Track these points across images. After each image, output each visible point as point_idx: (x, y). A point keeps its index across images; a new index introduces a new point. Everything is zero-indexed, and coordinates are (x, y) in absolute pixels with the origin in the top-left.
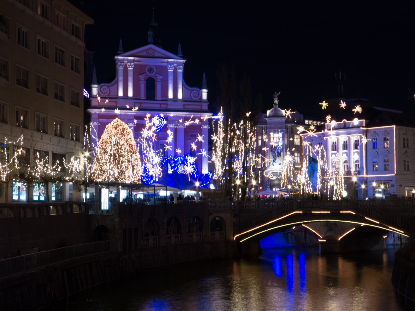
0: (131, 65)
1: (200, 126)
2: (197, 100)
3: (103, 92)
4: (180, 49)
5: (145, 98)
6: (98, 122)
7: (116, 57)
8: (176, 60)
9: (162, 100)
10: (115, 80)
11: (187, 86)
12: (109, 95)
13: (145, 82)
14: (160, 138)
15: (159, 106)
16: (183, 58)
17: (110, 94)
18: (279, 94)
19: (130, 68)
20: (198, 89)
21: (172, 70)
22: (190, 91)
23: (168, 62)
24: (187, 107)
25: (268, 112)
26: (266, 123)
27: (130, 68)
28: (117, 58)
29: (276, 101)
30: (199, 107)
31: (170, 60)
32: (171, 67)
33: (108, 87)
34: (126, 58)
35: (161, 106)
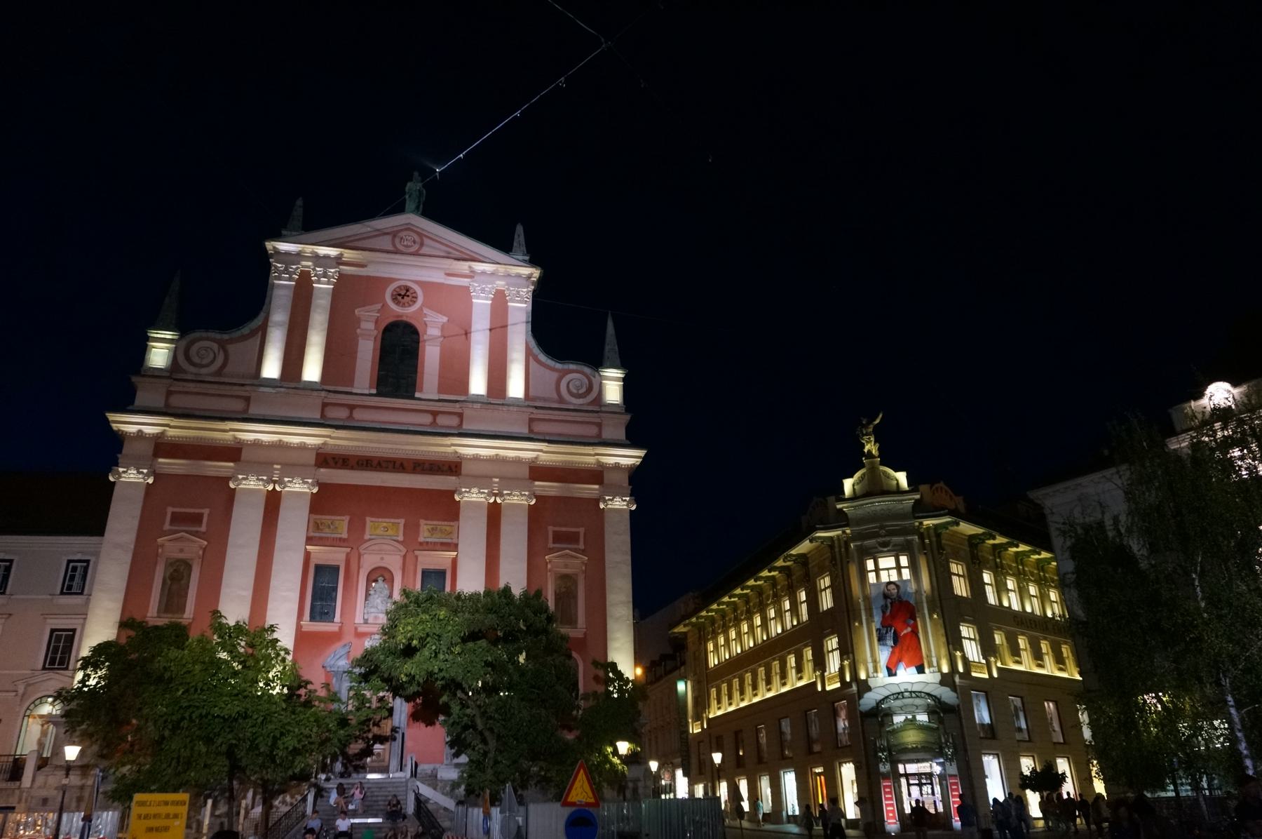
0: (325, 275)
1: (597, 501)
2: (585, 408)
3: (196, 360)
4: (522, 239)
5: (374, 391)
7: (270, 245)
8: (501, 269)
9: (439, 400)
10: (258, 322)
11: (543, 357)
12: (219, 372)
14: (421, 544)
15: (427, 419)
16: (533, 262)
17: (226, 370)
18: (877, 421)
19: (323, 287)
20: (587, 370)
21: (486, 299)
22: (555, 375)
23: (472, 275)
25: (848, 485)
26: (841, 519)
27: (323, 287)
28: (274, 248)
29: (871, 447)
30: (593, 431)
31: (479, 267)
32: (483, 290)
33: (223, 345)
34: (309, 249)
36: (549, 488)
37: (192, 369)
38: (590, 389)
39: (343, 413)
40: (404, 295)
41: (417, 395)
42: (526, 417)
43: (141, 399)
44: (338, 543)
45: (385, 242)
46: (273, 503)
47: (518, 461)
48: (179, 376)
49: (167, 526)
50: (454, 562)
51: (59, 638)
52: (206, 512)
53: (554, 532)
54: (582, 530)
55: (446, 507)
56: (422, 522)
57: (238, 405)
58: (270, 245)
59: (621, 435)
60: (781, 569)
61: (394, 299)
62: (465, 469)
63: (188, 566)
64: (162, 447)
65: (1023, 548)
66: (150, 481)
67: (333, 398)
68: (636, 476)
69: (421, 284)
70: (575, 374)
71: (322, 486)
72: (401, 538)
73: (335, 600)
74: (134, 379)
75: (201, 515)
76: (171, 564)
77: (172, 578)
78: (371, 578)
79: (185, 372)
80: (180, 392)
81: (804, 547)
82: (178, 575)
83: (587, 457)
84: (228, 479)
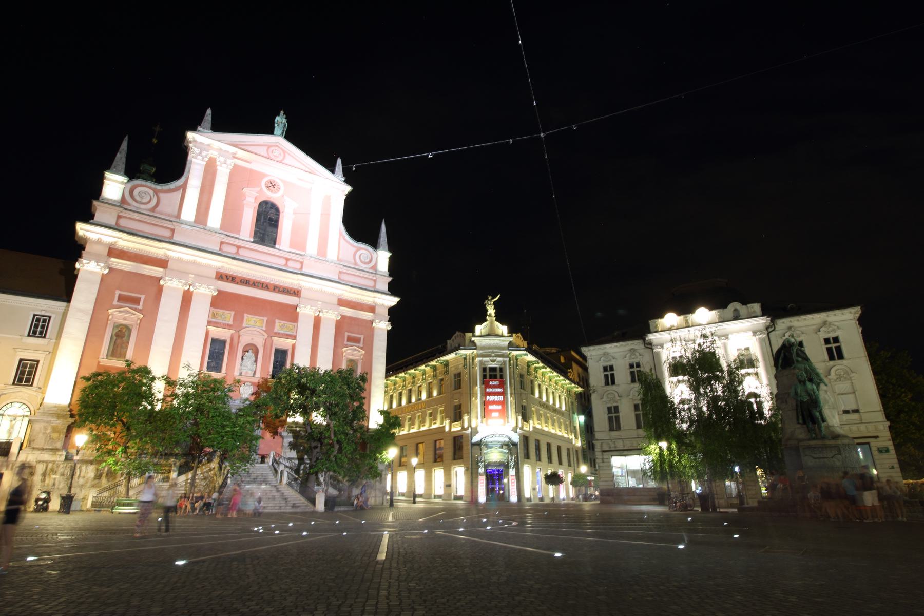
3: (137, 198)
6: (102, 265)
7: (190, 135)
11: (348, 238)
12: (153, 209)
13: (256, 205)
15: (283, 262)
17: (158, 209)
20: (370, 249)
22: (354, 249)
24: (345, 277)
26: (473, 345)
29: (491, 310)
30: (371, 284)
33: (156, 192)
35: (286, 265)
36: (349, 312)
37: (134, 204)
38: (371, 261)
39: (234, 250)
40: (272, 185)
41: (277, 246)
42: (338, 270)
43: (97, 218)
44: (228, 326)
45: (263, 151)
46: (187, 299)
47: (332, 294)
48: (126, 206)
49: (115, 302)
50: (294, 346)
51: (25, 366)
52: (143, 297)
53: (348, 337)
54: (362, 337)
55: (291, 313)
56: (277, 321)
57: (167, 233)
58: (190, 135)
59: (385, 288)
60: (432, 367)
61: (268, 187)
62: (303, 294)
63: (128, 329)
64: (114, 252)
65: (548, 369)
66: (106, 271)
67: (227, 240)
68: (392, 311)
69: (284, 182)
70: (364, 249)
71: (220, 292)
72: (264, 328)
73: (222, 360)
74: (95, 203)
75: (140, 299)
76: (117, 327)
77: (117, 335)
78: (246, 351)
79: (129, 204)
80: (126, 218)
81: (450, 357)
82: (121, 335)
83: (368, 298)
84: (159, 279)
